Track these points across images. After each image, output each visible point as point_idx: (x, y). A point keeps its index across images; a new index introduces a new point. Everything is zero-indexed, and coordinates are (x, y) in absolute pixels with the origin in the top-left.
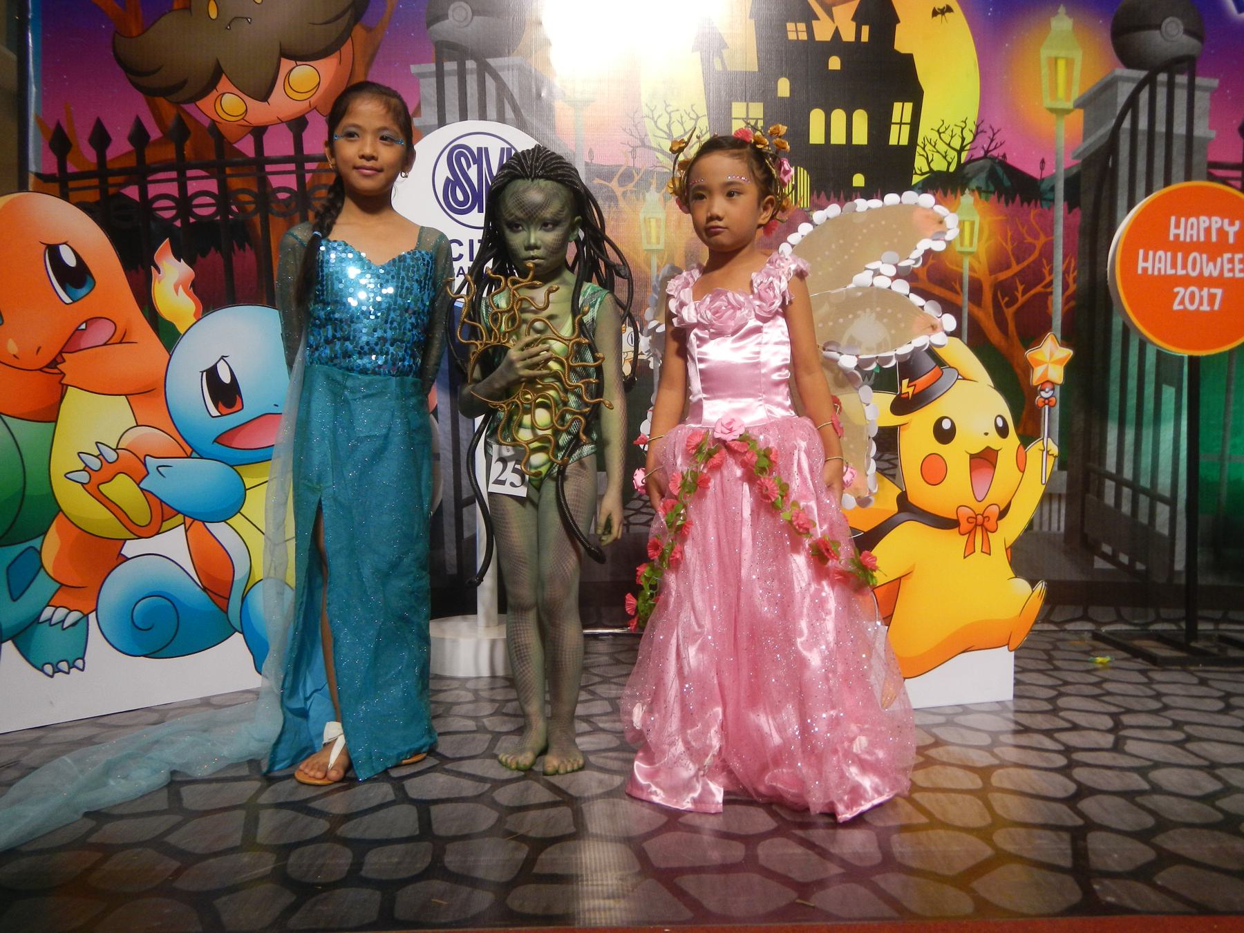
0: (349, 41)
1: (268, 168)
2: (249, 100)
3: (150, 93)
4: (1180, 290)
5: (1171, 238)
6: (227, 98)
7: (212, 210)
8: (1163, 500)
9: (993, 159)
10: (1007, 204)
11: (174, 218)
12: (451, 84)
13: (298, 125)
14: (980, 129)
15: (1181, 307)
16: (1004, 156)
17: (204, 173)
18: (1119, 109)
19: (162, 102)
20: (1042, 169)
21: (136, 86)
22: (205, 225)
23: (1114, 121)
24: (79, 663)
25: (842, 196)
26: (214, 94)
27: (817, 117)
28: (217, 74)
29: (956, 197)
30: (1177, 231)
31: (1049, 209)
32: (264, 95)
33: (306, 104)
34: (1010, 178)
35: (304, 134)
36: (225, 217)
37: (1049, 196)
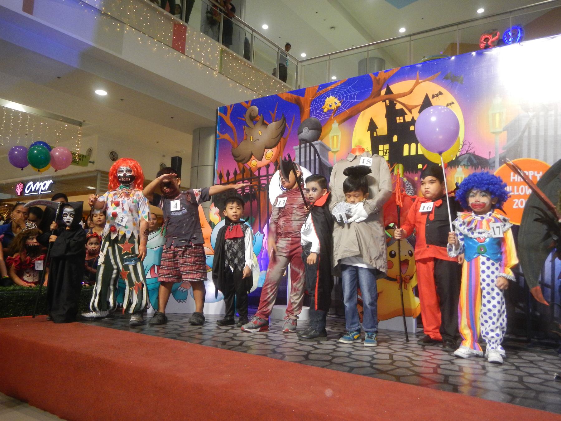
0: (280, 143)
1: (261, 178)
2: (258, 161)
3: (238, 162)
4: (517, 200)
5: (512, 180)
6: (254, 161)
7: (249, 190)
8: (547, 286)
9: (470, 154)
10: (475, 169)
11: (241, 193)
12: (303, 150)
13: (268, 166)
14: (465, 143)
15: (517, 207)
16: (474, 152)
17: (248, 181)
18: (523, 128)
19: (240, 164)
20: (490, 155)
21: (236, 160)
22: (247, 194)
23: (520, 134)
24: (185, 300)
25: (414, 172)
26: (251, 160)
27: (406, 146)
28: (252, 154)
29: (455, 169)
30: (514, 178)
31: (493, 170)
32: (261, 160)
33: (269, 161)
34: (476, 160)
35: (269, 169)
36: (251, 193)
37: (493, 165)
